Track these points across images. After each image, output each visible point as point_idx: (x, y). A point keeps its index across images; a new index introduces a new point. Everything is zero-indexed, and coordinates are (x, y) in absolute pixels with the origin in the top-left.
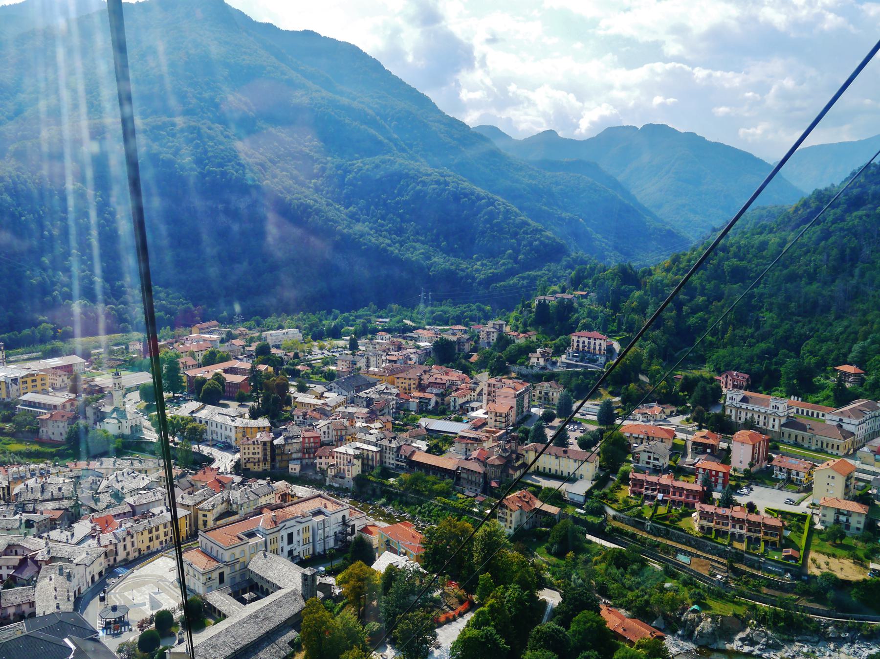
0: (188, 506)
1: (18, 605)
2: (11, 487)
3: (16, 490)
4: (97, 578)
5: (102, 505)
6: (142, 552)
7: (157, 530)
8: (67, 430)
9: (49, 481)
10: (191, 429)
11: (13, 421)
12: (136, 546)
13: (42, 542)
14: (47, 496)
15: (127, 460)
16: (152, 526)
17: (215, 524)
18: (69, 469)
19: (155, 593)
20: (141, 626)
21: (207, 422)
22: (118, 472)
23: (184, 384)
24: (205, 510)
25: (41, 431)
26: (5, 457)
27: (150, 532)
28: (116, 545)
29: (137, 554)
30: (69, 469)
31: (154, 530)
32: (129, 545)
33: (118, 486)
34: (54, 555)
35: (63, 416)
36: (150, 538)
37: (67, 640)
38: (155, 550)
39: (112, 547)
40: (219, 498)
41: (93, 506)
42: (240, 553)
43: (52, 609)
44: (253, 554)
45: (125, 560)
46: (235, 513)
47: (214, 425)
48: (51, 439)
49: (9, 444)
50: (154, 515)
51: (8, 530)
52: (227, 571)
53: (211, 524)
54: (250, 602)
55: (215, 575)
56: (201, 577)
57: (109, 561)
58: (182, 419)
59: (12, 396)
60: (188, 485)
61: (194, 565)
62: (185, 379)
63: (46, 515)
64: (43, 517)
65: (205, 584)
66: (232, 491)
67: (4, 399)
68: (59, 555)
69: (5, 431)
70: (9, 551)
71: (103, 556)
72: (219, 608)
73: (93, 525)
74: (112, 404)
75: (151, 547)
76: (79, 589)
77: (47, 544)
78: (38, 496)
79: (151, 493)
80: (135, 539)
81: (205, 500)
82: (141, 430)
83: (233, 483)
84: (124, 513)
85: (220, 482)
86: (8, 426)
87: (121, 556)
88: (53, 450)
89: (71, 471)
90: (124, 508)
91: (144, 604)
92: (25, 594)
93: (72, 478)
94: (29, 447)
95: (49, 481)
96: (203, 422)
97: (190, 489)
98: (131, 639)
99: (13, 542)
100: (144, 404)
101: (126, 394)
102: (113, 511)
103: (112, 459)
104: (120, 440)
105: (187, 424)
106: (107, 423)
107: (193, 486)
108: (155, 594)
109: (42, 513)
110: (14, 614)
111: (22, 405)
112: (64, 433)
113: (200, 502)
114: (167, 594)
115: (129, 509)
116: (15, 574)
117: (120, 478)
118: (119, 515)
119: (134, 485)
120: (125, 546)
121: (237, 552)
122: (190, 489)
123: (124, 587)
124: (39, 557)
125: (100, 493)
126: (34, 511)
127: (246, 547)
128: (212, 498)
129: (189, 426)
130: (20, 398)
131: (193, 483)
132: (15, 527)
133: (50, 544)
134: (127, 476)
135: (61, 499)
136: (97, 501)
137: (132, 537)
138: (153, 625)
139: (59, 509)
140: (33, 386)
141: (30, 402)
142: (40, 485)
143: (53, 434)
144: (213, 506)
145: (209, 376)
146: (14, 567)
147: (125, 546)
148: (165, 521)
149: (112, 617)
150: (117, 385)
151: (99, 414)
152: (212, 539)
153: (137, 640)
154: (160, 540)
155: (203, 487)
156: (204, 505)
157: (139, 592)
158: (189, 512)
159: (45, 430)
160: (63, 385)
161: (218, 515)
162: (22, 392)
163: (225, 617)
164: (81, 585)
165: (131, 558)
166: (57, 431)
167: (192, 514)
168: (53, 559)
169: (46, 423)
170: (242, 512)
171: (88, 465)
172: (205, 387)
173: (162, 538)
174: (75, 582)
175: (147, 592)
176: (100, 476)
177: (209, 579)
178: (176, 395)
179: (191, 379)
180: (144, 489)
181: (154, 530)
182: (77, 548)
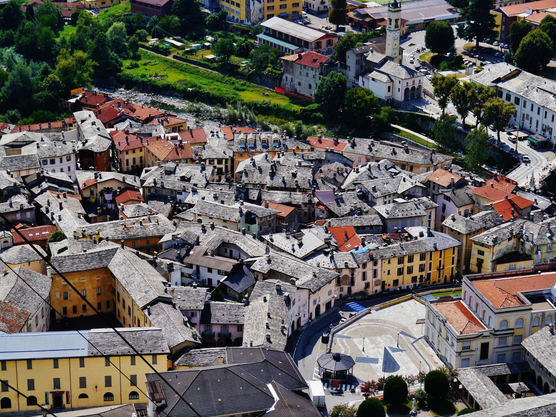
0: (459, 233)
1: (225, 326)
2: (237, 159)
3: (243, 165)
4: (323, 310)
5: (346, 208)
6: (386, 287)
7: (411, 260)
8: (319, 82)
9: (282, 159)
10: (490, 108)
11: (251, 57)
12: (379, 277)
13: (262, 247)
14: (277, 182)
15: (388, 145)
16: (404, 253)
17: (494, 269)
18: (309, 147)
19: (394, 350)
20: (366, 389)
21: (517, 101)
22: (373, 164)
23: (495, 29)
24: (483, 245)
25: (284, 77)
26: (236, 108)
27: (401, 261)
28: (353, 270)
29: (379, 288)
30: (309, 147)
31: (406, 259)
32: (370, 274)
33: (369, 185)
34: (274, 267)
35: (315, 61)
36: (399, 269)
37: (270, 386)
38: (404, 287)
39: (346, 272)
40: (505, 231)
41: (333, 207)
42: (517, 323)
43: (260, 341)
44: (534, 328)
45: (361, 293)
46: (527, 257)
47: (529, 106)
48: (296, 91)
49: (243, 90)
50: (410, 236)
51: (224, 221)
52: (493, 343)
53: (487, 267)
54: (518, 396)
55: (476, 345)
56: (455, 342)
57: (342, 290)
58: (481, 89)
59: (253, 18)
60: (467, 200)
61: (448, 324)
62: (498, 20)
63: (273, 209)
64: (268, 212)
65: (459, 353)
66: (529, 223)
67: (242, 22)
68: (280, 270)
69: (240, 70)
70: (223, 249)
71: (334, 282)
72: (471, 393)
73: (327, 236)
74: (382, 50)
75: (400, 282)
76: (299, 320)
77: (267, 251)
78: (267, 180)
79: (411, 205)
80: (378, 267)
81: (485, 229)
83: (534, 208)
84: (371, 227)
85: (513, 204)
86: (244, 63)
87: (359, 286)
88: (296, 108)
89: (312, 150)
90: (373, 220)
91: (375, 361)
92: (233, 312)
93: (311, 161)
94: (267, 100)
95: (282, 159)
96: (513, 100)
97: (469, 207)
98: (350, 405)
99: (228, 239)
100: (429, 55)
101: (408, 33)
102: (356, 221)
103: (369, 141)
104: (387, 108)
105: (484, 100)
106: (373, 79)
107: (473, 202)
108: (394, 350)
109: (267, 207)
110: (219, 335)
111: (265, 34)
112: (313, 86)
113: (478, 231)
114: (409, 355)
115: (378, 222)
116: (227, 283)
117: (375, 173)
118: (363, 227)
119: (390, 188)
120: (364, 274)
121: (512, 319)
122: (469, 207)
123: (356, 332)
124: (256, 267)
125: (344, 190)
126: (259, 201)
127: (527, 316)
128: (495, 229)
129: (488, 104)
130: (262, 24)
131: (474, 198)
132: (233, 219)
133: (272, 252)
134: (383, 172)
135: (294, 190)
136: (339, 201)
137: (375, 264)
138: (381, 393)
139: (289, 204)
140: (282, 7)
141: (274, 31)
142: (269, 165)
143: (300, 84)
144: (495, 241)
145: (537, 19)
146: (226, 273)
147: (364, 274)
148: (423, 251)
149: (332, 366)
150: (393, 23)
151: (364, 64)
152: (479, 292)
153: (357, 407)
154: (414, 275)
155: (486, 208)
156: (485, 237)
157: (373, 342)
158: (456, 243)
159: (289, 77)
160: (322, 8)
161: (500, 255)
162: (267, 13)
163: (478, 408)
164: (301, 315)
165: (371, 291)
166: (305, 81)
167: (464, 248)
168: (272, 274)
169: (292, 67)
170: (538, 257)
171: (337, 143)
172: (526, 39)
173: (416, 273)
174: (294, 309)
175: (383, 345)
176: (348, 163)
177: (467, 349)
178: (481, 44)
179: (509, 20)
180: (403, 195)
181: (406, 259)
182: (302, 264)
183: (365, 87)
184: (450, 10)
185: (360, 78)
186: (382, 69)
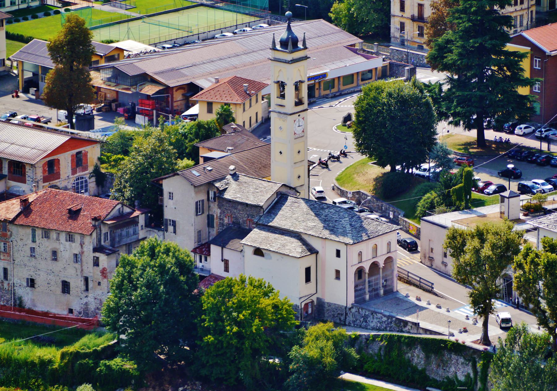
23: (523, 91)
35: (74, 214)
48: (19, 305)
82: (390, 292)
106: (258, 252)
143: (32, 283)
150: (290, 91)
183: (233, 274)
184: (351, 48)
185: (215, 250)
186: (277, 222)
